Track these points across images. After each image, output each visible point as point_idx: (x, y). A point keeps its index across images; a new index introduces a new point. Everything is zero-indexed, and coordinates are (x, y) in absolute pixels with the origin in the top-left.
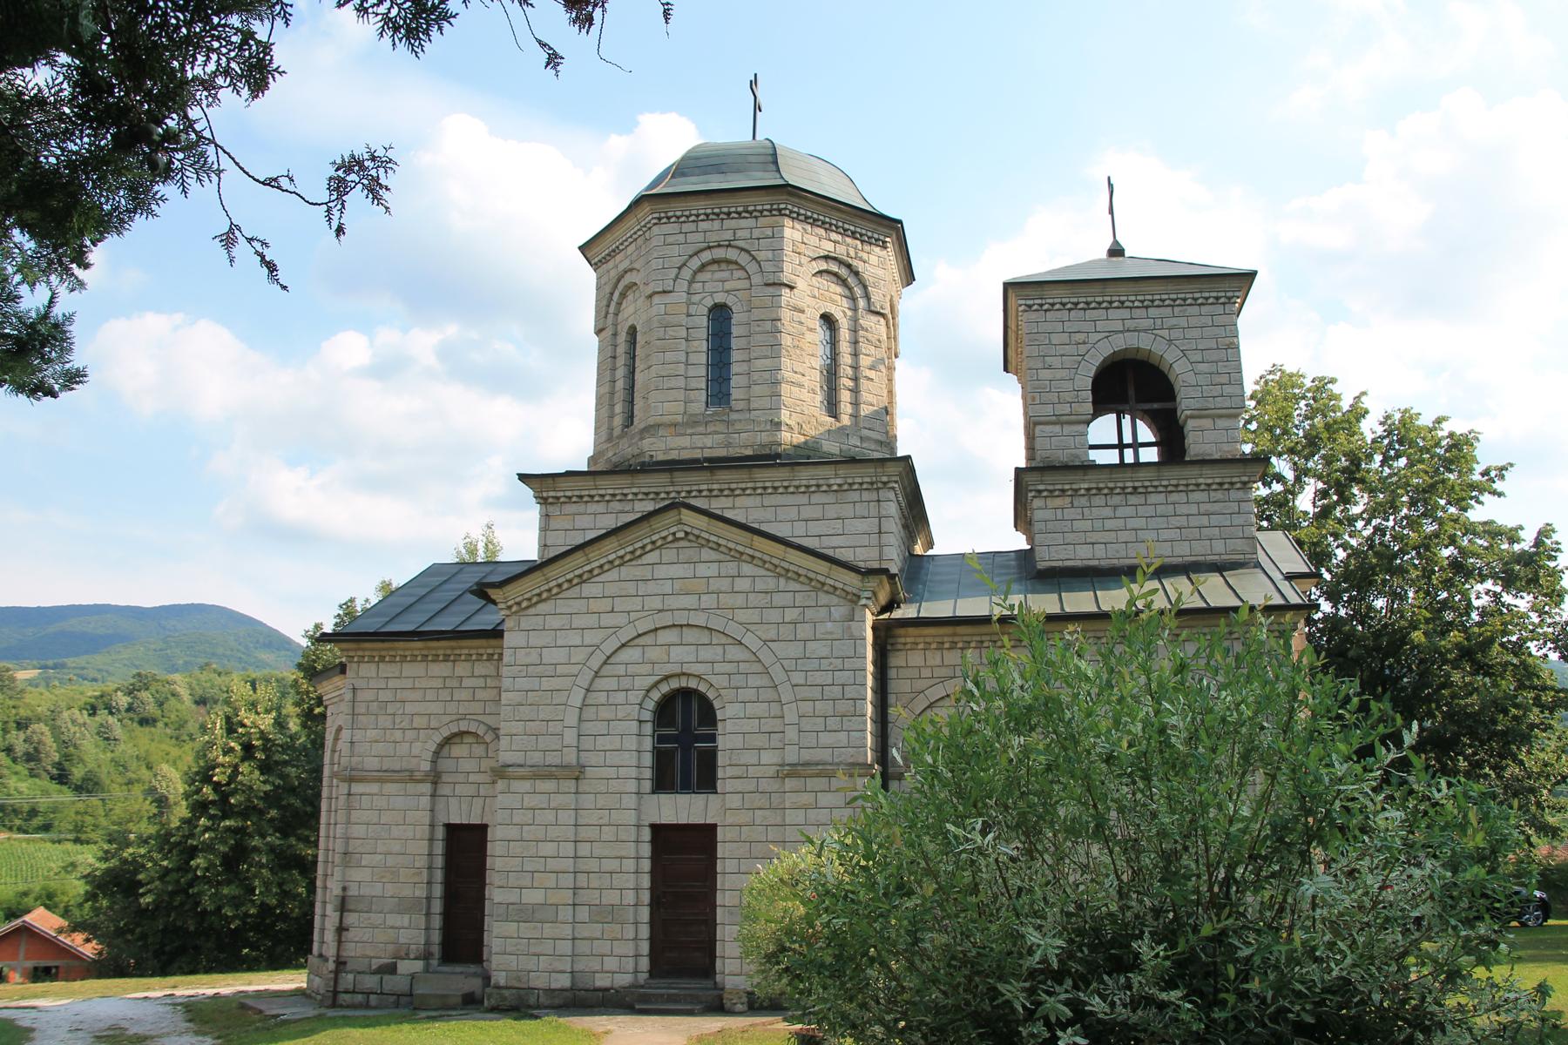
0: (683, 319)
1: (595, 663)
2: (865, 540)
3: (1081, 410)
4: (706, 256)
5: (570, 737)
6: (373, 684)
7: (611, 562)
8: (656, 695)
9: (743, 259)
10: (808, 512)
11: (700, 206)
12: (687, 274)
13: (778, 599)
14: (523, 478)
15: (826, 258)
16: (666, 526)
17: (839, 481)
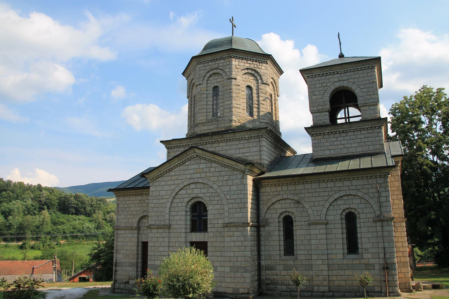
0: (205, 92)
1: (173, 195)
2: (256, 153)
3: (326, 108)
4: (211, 73)
5: (167, 216)
6: (123, 203)
7: (177, 165)
8: (190, 203)
9: (221, 72)
10: (239, 146)
11: (208, 58)
12: (206, 78)
13: (222, 174)
14: (161, 142)
15: (247, 69)
16: (191, 154)
17: (248, 136)
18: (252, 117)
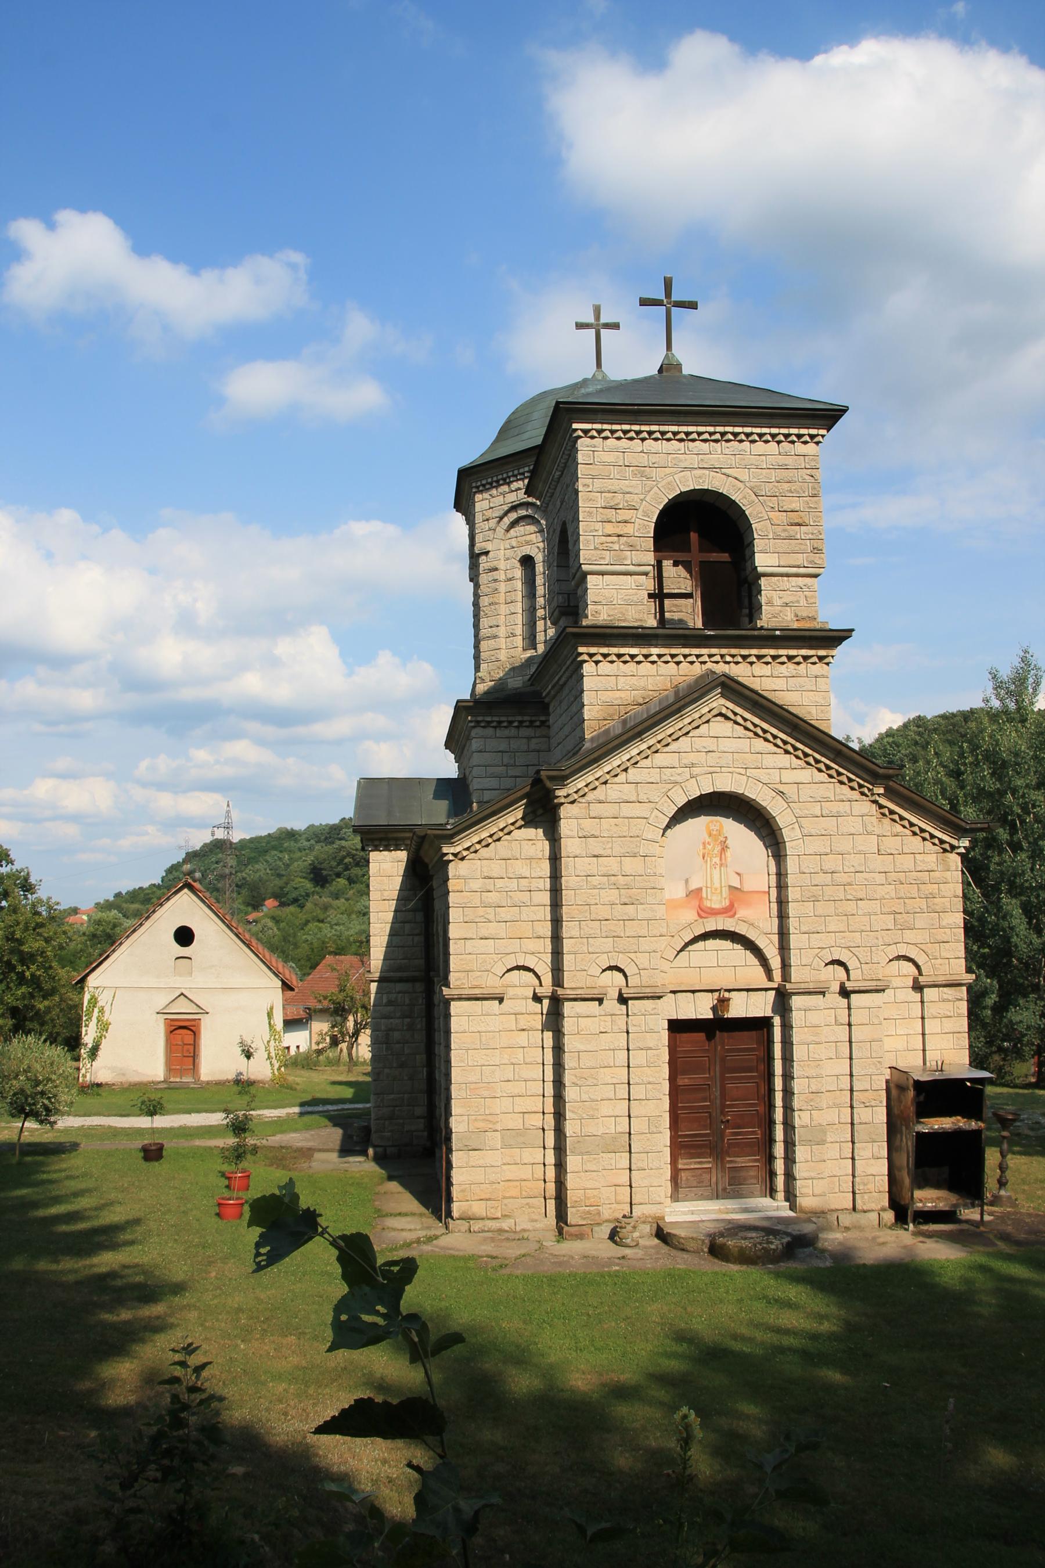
15: (514, 508)
18: (535, 649)
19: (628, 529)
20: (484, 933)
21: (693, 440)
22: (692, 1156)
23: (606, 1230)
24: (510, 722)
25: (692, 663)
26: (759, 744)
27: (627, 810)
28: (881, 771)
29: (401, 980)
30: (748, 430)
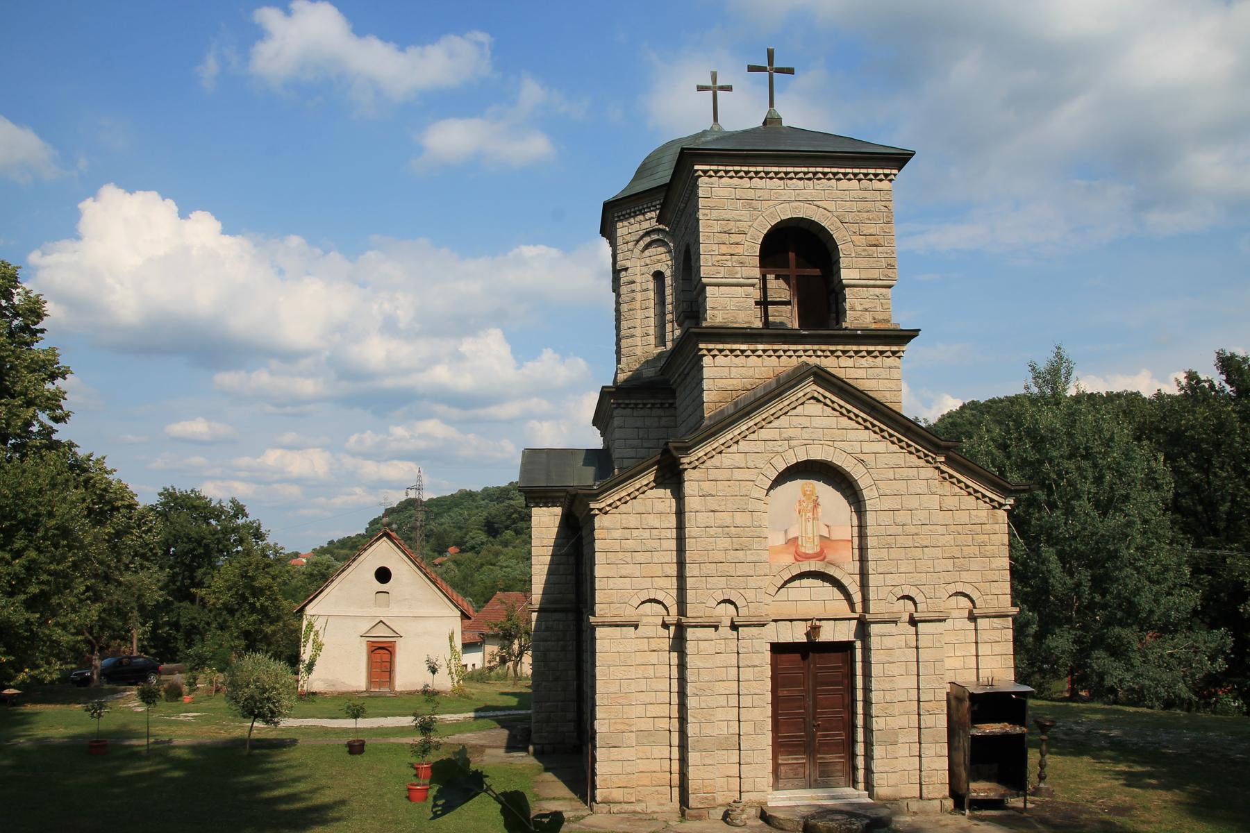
15: (648, 233)
19: (740, 249)
20: (623, 573)
21: (791, 179)
22: (790, 753)
23: (720, 813)
24: (645, 404)
25: (790, 357)
26: (844, 422)
27: (738, 474)
28: (942, 443)
29: (556, 611)
30: (835, 170)
